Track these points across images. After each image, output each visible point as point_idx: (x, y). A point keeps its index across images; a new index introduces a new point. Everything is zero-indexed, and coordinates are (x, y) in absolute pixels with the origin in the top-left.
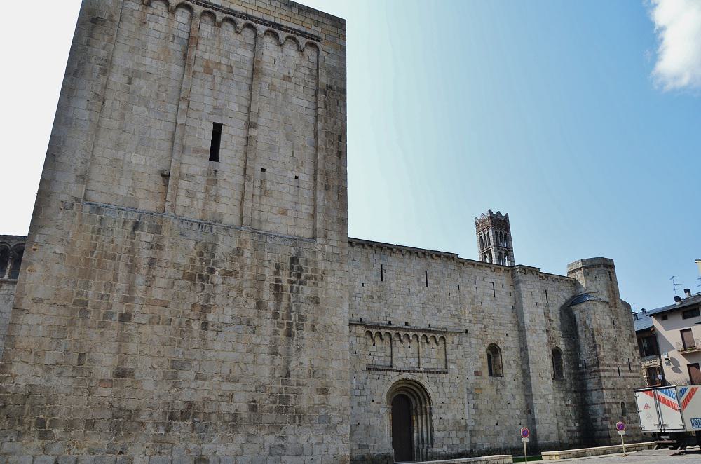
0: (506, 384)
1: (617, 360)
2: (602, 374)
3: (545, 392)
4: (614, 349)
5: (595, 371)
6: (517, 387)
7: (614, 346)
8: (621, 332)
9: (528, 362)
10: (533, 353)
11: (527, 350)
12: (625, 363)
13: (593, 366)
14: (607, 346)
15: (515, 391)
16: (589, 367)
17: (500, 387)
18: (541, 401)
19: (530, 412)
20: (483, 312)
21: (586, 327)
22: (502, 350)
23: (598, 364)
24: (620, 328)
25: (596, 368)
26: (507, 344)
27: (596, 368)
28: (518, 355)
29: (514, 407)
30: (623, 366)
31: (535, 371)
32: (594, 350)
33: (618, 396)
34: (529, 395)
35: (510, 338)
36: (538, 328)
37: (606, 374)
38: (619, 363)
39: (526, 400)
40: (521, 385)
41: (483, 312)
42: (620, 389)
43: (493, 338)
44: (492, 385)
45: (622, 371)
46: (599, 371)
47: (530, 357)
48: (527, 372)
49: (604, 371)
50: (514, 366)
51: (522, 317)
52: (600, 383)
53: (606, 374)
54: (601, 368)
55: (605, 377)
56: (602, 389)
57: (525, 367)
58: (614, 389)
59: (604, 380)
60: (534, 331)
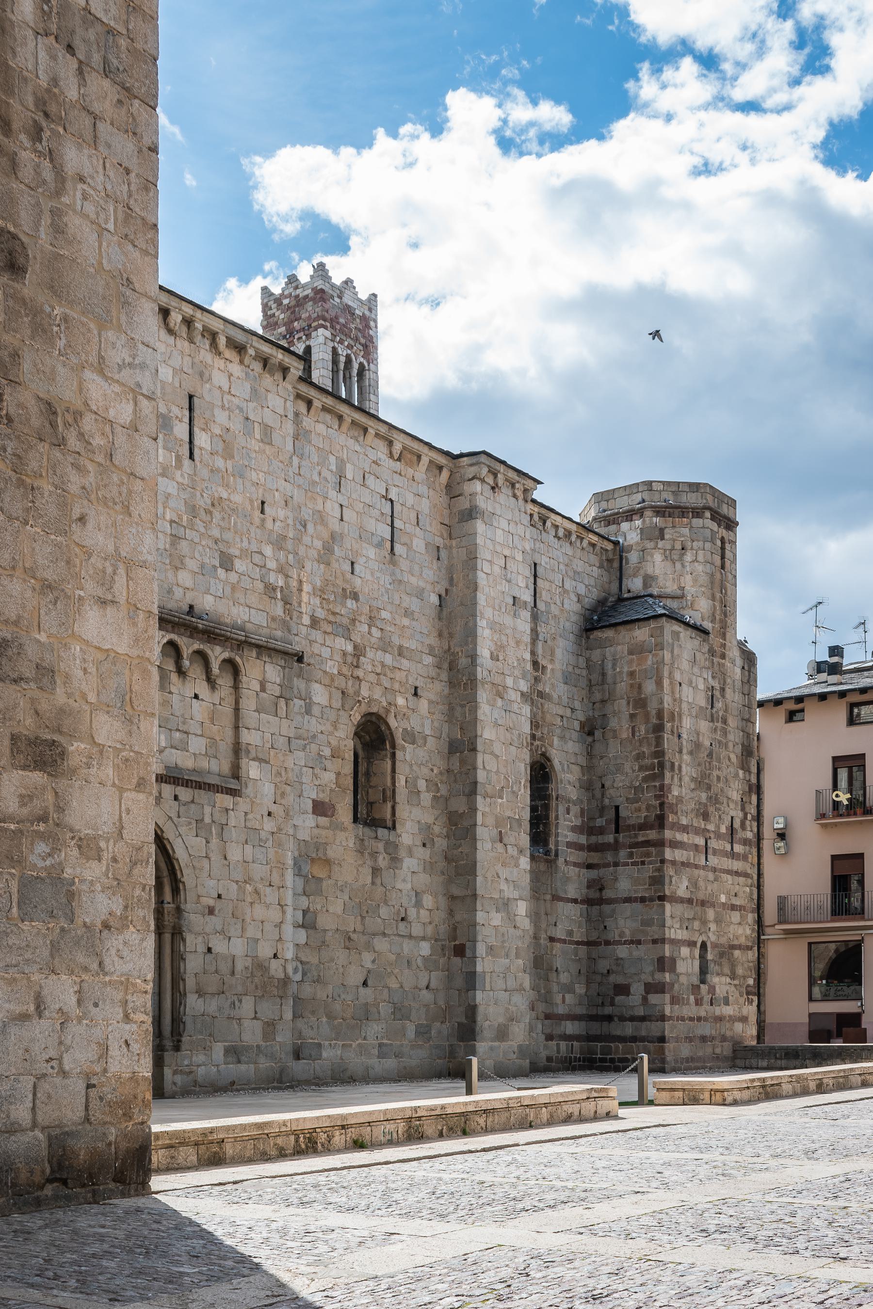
0: (402, 853)
1: (706, 816)
2: (668, 854)
3: (509, 892)
4: (702, 782)
5: (647, 843)
6: (429, 867)
7: (704, 775)
8: (725, 733)
9: (472, 790)
10: (492, 765)
11: (474, 750)
12: (723, 830)
13: (643, 827)
14: (688, 770)
15: (424, 879)
16: (630, 828)
17: (383, 861)
18: (497, 919)
19: (460, 951)
20: (355, 596)
21: (641, 703)
22: (399, 741)
23: (660, 822)
24: (725, 721)
25: (652, 835)
26: (414, 723)
27: (652, 835)
28: (440, 764)
29: (417, 930)
30: (719, 836)
31: (490, 821)
32: (653, 777)
33: (696, 924)
34: (463, 898)
35: (423, 705)
36: (509, 682)
37: (679, 855)
38: (711, 827)
39: (451, 913)
40: (442, 864)
41: (355, 596)
42: (703, 903)
43: (377, 694)
44: (361, 852)
45: (715, 852)
46: (660, 844)
47: (481, 776)
48: (466, 823)
49: (675, 845)
50: (426, 798)
51: (471, 635)
52: (658, 880)
53: (679, 855)
54: (668, 834)
55: (673, 863)
56: (662, 898)
57: (459, 805)
58: (690, 901)
59: (669, 871)
60: (500, 692)
